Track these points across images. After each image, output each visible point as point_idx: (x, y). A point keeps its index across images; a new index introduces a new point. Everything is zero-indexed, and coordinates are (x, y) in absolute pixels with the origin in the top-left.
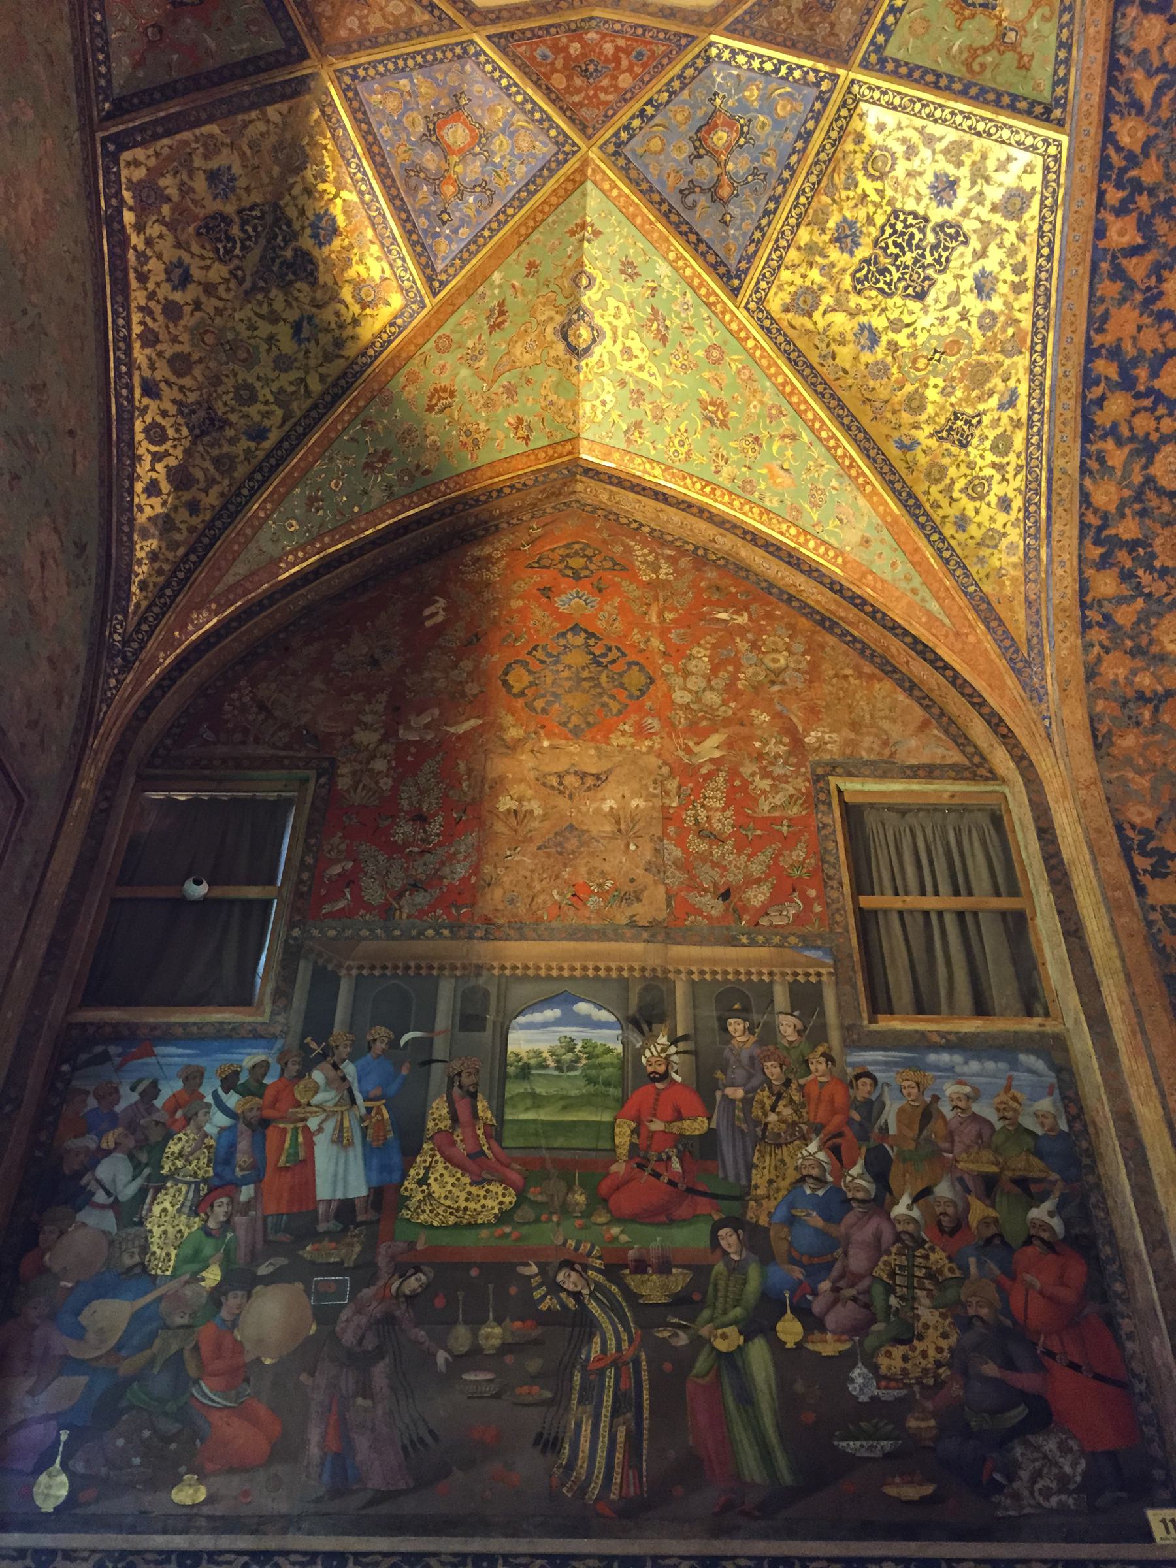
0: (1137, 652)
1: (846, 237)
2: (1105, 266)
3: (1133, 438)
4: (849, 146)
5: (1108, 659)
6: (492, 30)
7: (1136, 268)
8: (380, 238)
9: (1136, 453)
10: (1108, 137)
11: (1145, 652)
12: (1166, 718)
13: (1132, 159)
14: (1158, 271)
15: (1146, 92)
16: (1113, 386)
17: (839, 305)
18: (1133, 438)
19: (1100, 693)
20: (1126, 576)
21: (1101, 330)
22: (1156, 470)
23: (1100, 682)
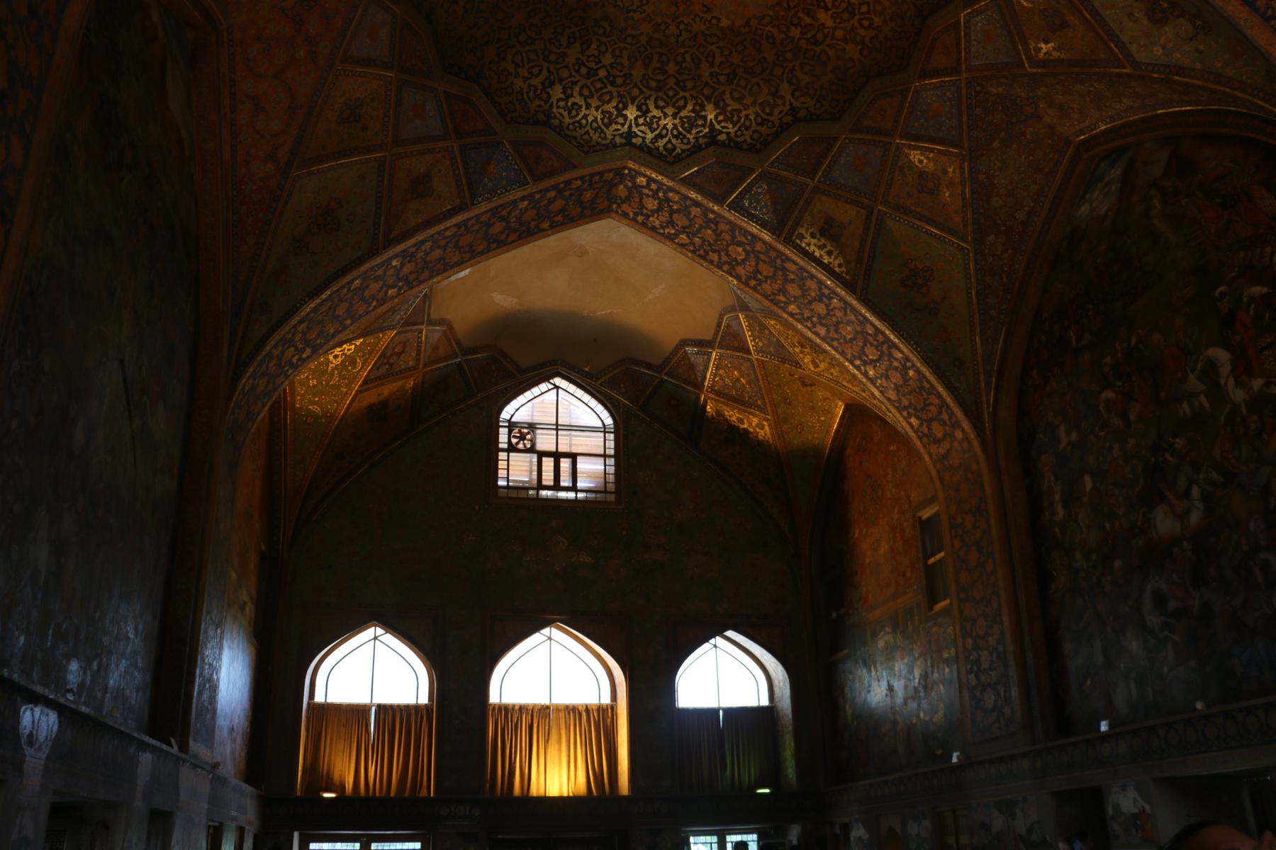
10: (791, 315)
14: (837, 331)
20: (917, 417)
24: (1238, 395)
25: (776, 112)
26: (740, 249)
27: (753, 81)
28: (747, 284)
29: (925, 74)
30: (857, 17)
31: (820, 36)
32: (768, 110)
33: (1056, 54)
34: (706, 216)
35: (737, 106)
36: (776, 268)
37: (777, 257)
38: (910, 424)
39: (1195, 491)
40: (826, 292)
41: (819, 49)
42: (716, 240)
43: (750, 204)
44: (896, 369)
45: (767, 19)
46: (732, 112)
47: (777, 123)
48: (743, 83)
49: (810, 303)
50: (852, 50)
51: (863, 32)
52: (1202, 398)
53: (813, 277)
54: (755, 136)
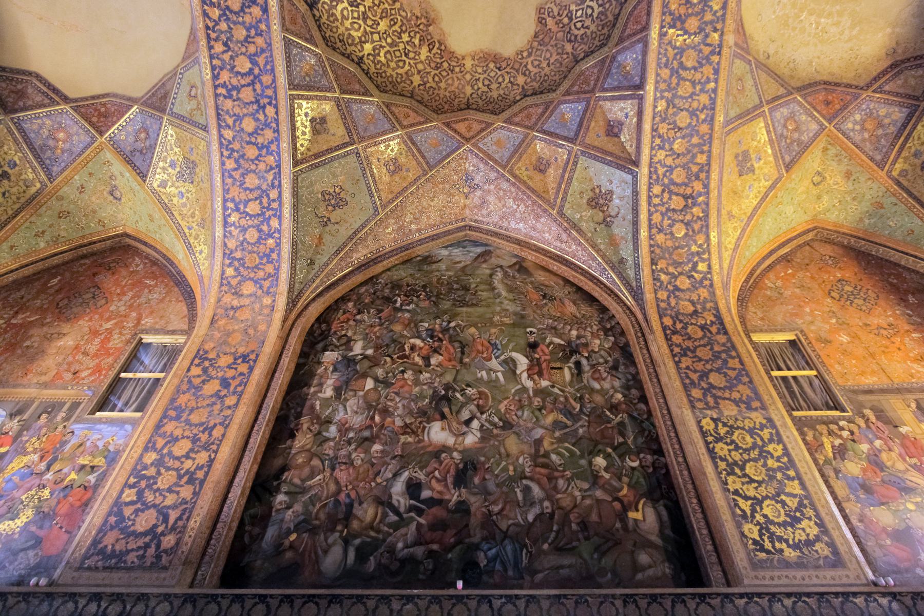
0: (236, 293)
1: (173, 165)
2: (226, 174)
3: (240, 226)
4: (169, 138)
5: (226, 296)
6: (72, 105)
7: (237, 175)
8: (31, 167)
9: (241, 231)
10: (221, 136)
11: (236, 294)
12: (237, 315)
13: (229, 141)
14: (243, 175)
15: (230, 121)
16: (233, 211)
17: (173, 186)
18: (240, 226)
19: (221, 307)
20: (236, 269)
21: (228, 193)
22: (247, 236)
23: (221, 303)
24: (529, 384)
25: (353, 48)
26: (249, 65)
27: (361, 22)
28: (216, 87)
29: (448, 125)
30: (437, 72)
31: (411, 55)
32: (350, 41)
33: (526, 178)
34: (260, 21)
35: (339, 17)
36: (257, 101)
37: (270, 97)
38: (223, 273)
39: (475, 424)
40: (274, 147)
41: (404, 58)
42: (238, 42)
43: (295, 55)
44: (260, 231)
45: (404, 14)
46: (333, 14)
47: (348, 52)
48: (356, 15)
49: (249, 143)
50: (417, 80)
51: (430, 80)
52: (500, 375)
53: (277, 131)
54: (333, 39)
